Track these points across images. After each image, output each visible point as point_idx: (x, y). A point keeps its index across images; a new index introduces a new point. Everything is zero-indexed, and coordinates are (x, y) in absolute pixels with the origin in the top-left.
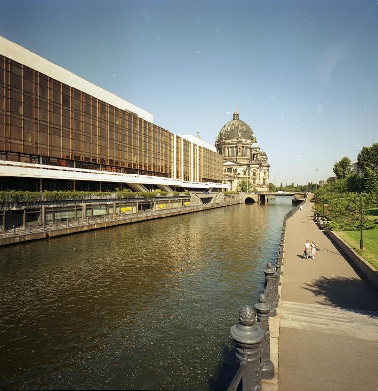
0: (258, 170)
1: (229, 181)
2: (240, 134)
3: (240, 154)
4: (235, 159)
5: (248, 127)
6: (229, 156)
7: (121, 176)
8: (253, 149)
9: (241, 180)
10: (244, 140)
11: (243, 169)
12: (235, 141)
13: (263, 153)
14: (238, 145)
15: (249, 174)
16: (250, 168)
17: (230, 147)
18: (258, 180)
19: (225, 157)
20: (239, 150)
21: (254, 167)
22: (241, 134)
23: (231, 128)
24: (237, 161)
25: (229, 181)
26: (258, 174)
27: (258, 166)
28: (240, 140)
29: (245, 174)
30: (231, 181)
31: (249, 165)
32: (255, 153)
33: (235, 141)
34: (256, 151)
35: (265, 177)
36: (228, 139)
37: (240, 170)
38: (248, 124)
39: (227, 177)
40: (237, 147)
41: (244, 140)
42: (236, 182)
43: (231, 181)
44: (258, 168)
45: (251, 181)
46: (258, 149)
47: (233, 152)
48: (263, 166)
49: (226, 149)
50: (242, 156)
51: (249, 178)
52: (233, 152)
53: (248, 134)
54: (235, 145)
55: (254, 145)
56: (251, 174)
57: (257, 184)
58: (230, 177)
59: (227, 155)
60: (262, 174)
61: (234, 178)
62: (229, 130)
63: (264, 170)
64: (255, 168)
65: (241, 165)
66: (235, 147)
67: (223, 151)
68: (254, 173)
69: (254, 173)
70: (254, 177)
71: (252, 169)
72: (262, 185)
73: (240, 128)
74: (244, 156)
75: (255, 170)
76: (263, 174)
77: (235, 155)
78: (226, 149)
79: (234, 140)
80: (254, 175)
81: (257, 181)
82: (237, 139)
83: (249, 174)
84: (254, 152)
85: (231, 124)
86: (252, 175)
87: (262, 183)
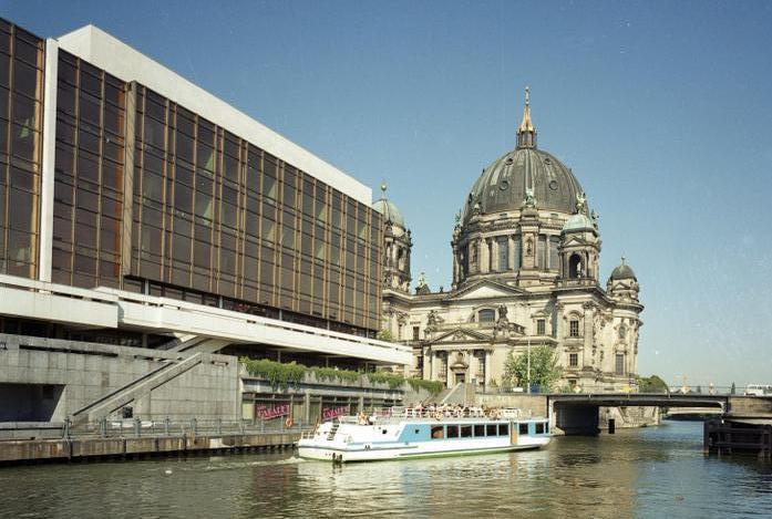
0: (589, 313)
1: (476, 352)
2: (530, 193)
3: (528, 262)
4: (511, 279)
5: (565, 173)
6: (491, 271)
7: (30, 294)
8: (569, 236)
9: (518, 352)
10: (544, 214)
11: (533, 311)
12: (514, 215)
13: (622, 269)
14: (524, 229)
15: (554, 332)
16: (560, 307)
17: (496, 238)
18: (588, 350)
19: (479, 272)
20: (526, 246)
21: (572, 304)
22: (535, 193)
23: (502, 172)
24: (517, 284)
25: (476, 352)
26: (588, 329)
27: (587, 297)
28: (530, 210)
29: (541, 330)
30: (481, 354)
31: (554, 295)
32: (579, 250)
33: (514, 215)
34: (582, 242)
35: (621, 347)
36: (491, 209)
37: (518, 314)
38: (568, 165)
39: (469, 338)
40: (518, 237)
41: (544, 214)
42: (499, 358)
43: (481, 354)
44: (588, 306)
45: (562, 359)
46: (589, 237)
47: (505, 256)
48: (613, 306)
49: (484, 246)
50: (535, 268)
51: (553, 344)
52: (505, 256)
53: (565, 193)
54: (513, 231)
55: (575, 222)
56: (563, 329)
57: (586, 368)
58: (480, 339)
59: (484, 267)
60: (608, 335)
61: (493, 341)
62: (495, 181)
63: (617, 321)
64: (578, 308)
65: (526, 297)
66: (513, 236)
67: (472, 253)
68: (574, 324)
69: (574, 324)
70: (573, 340)
71: (568, 309)
72: (610, 374)
73: (534, 173)
74: (547, 271)
75: (575, 313)
76: (615, 337)
77: (513, 263)
78: (484, 246)
79: (509, 215)
80: (574, 333)
81: (585, 356)
82: (521, 210)
83: (554, 332)
84: (572, 246)
85: (505, 160)
86: (566, 332)
87: (608, 365)
